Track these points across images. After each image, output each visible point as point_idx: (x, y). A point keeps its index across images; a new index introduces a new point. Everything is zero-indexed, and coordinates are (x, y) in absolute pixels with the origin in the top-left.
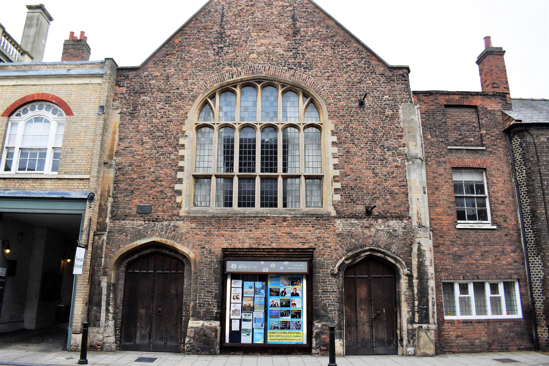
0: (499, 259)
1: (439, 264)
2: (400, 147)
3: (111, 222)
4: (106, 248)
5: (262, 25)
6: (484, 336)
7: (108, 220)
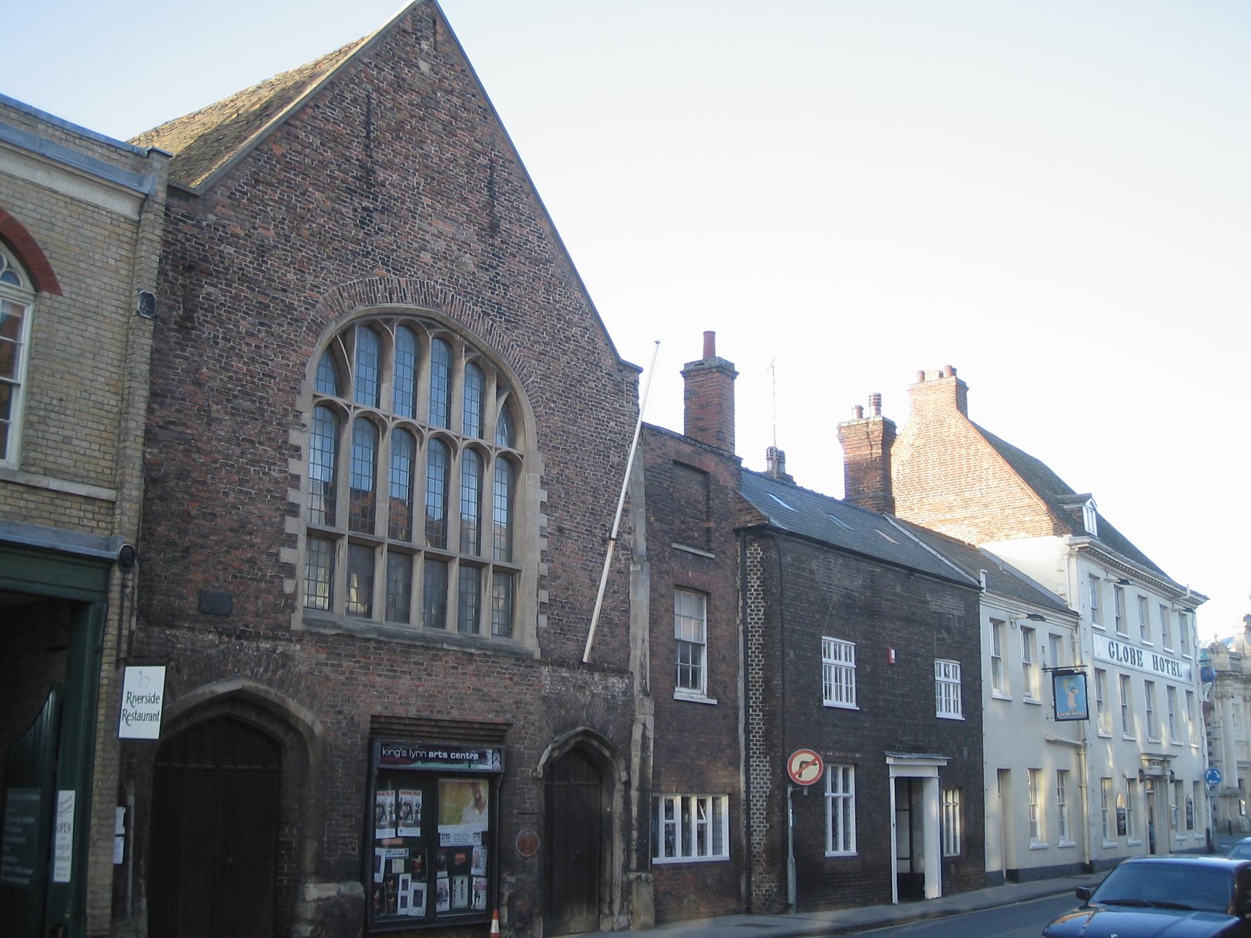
3: (140, 630)
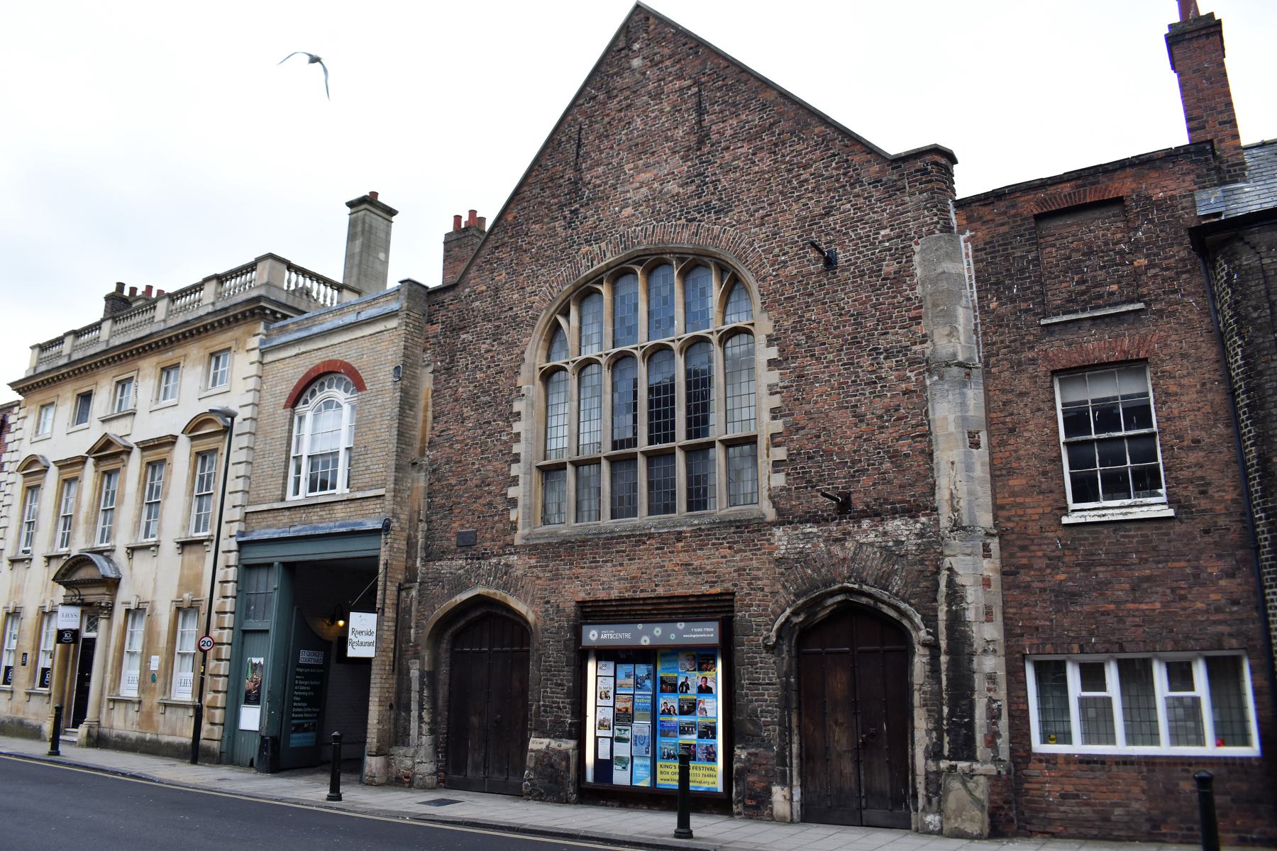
0: (1183, 598)
1: (1017, 617)
2: (915, 344)
4: (418, 611)
5: (643, 144)
6: (1137, 800)
7: (418, 564)
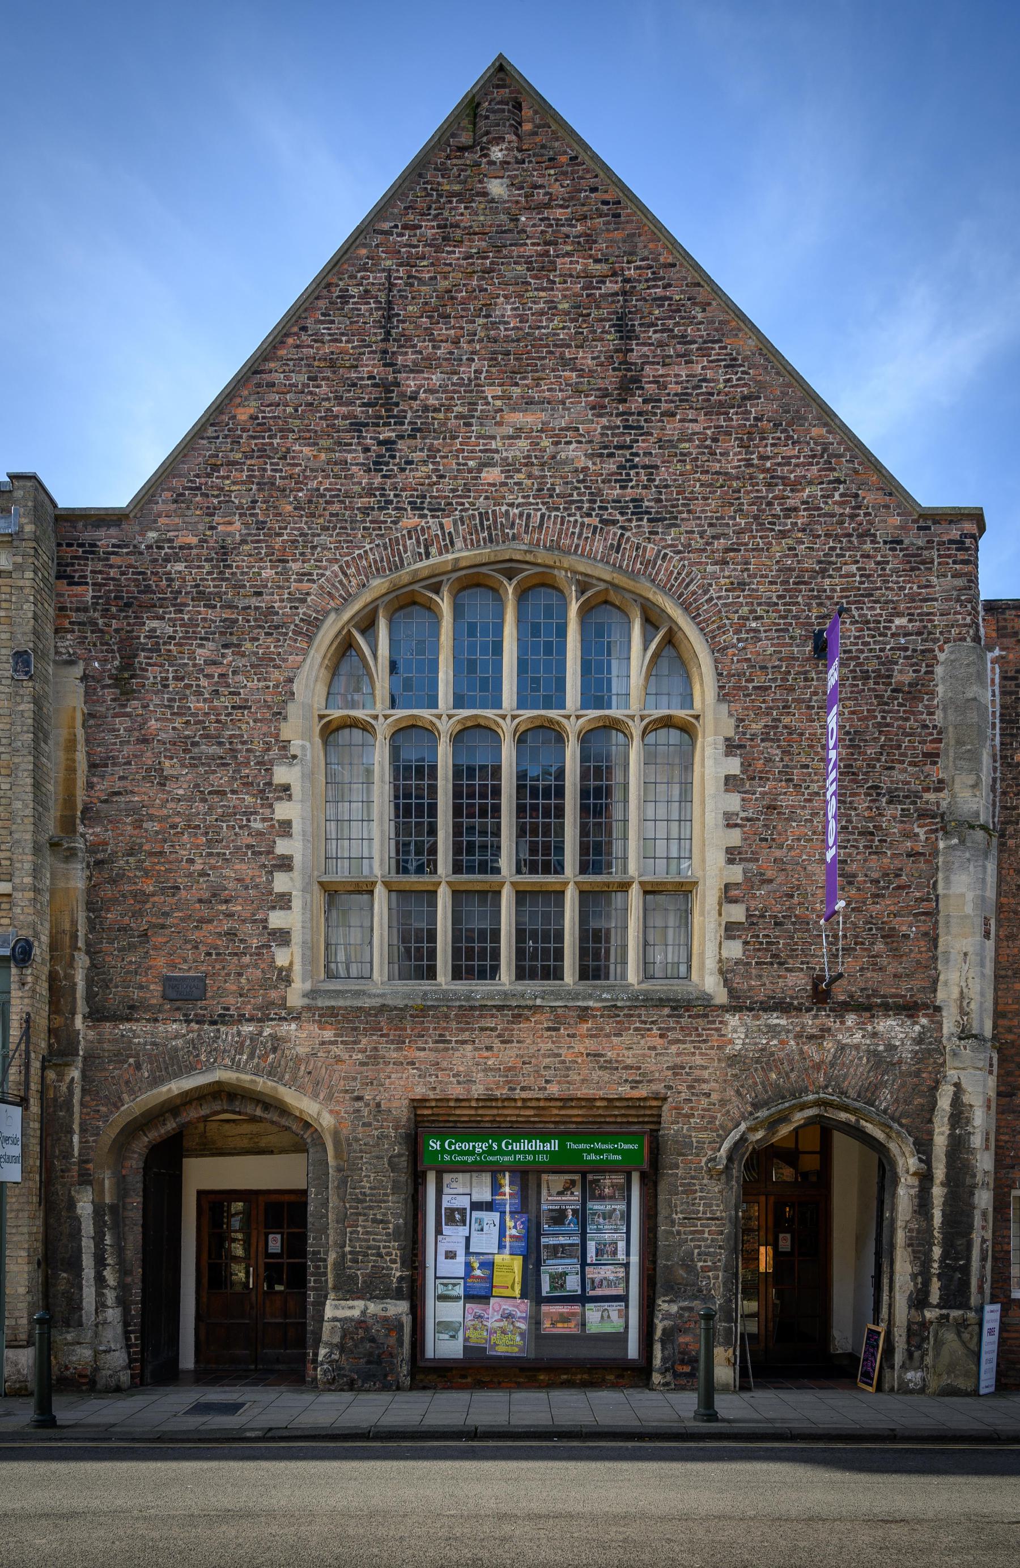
2: (927, 790)
7: (79, 1023)
